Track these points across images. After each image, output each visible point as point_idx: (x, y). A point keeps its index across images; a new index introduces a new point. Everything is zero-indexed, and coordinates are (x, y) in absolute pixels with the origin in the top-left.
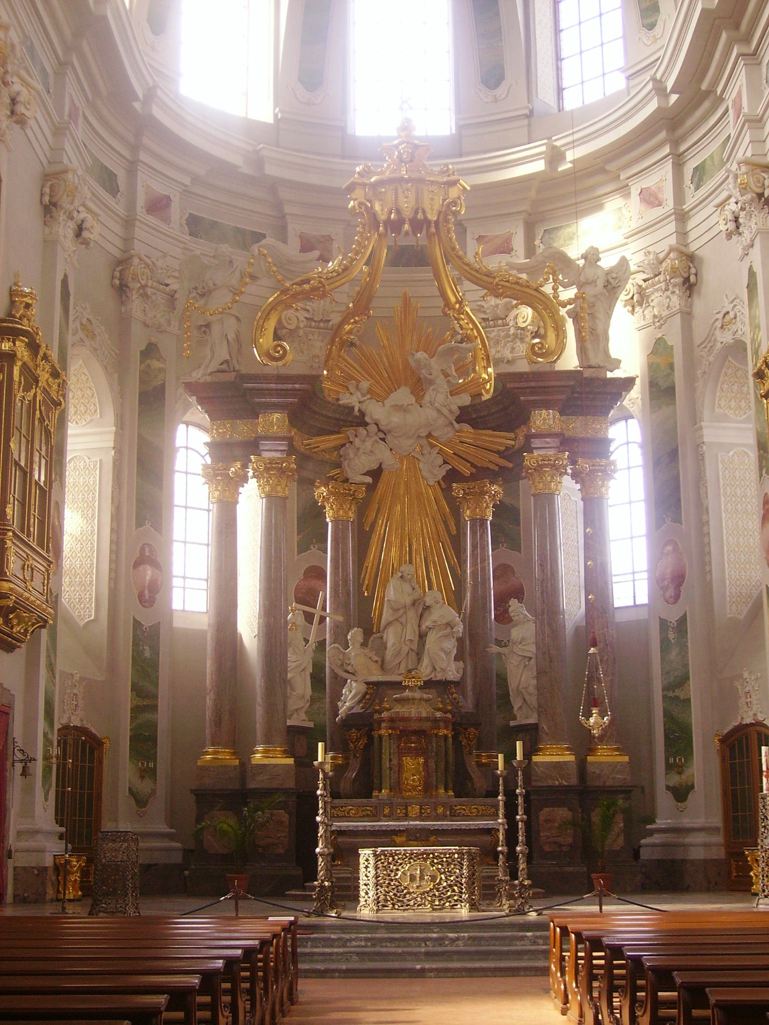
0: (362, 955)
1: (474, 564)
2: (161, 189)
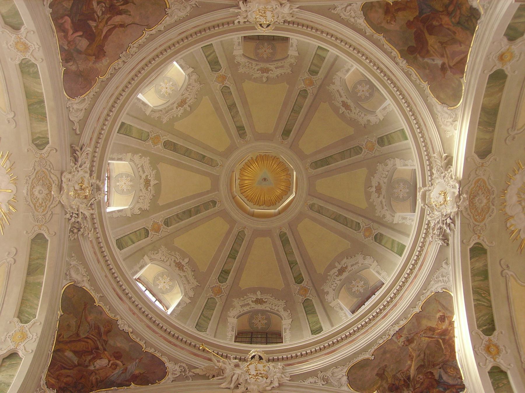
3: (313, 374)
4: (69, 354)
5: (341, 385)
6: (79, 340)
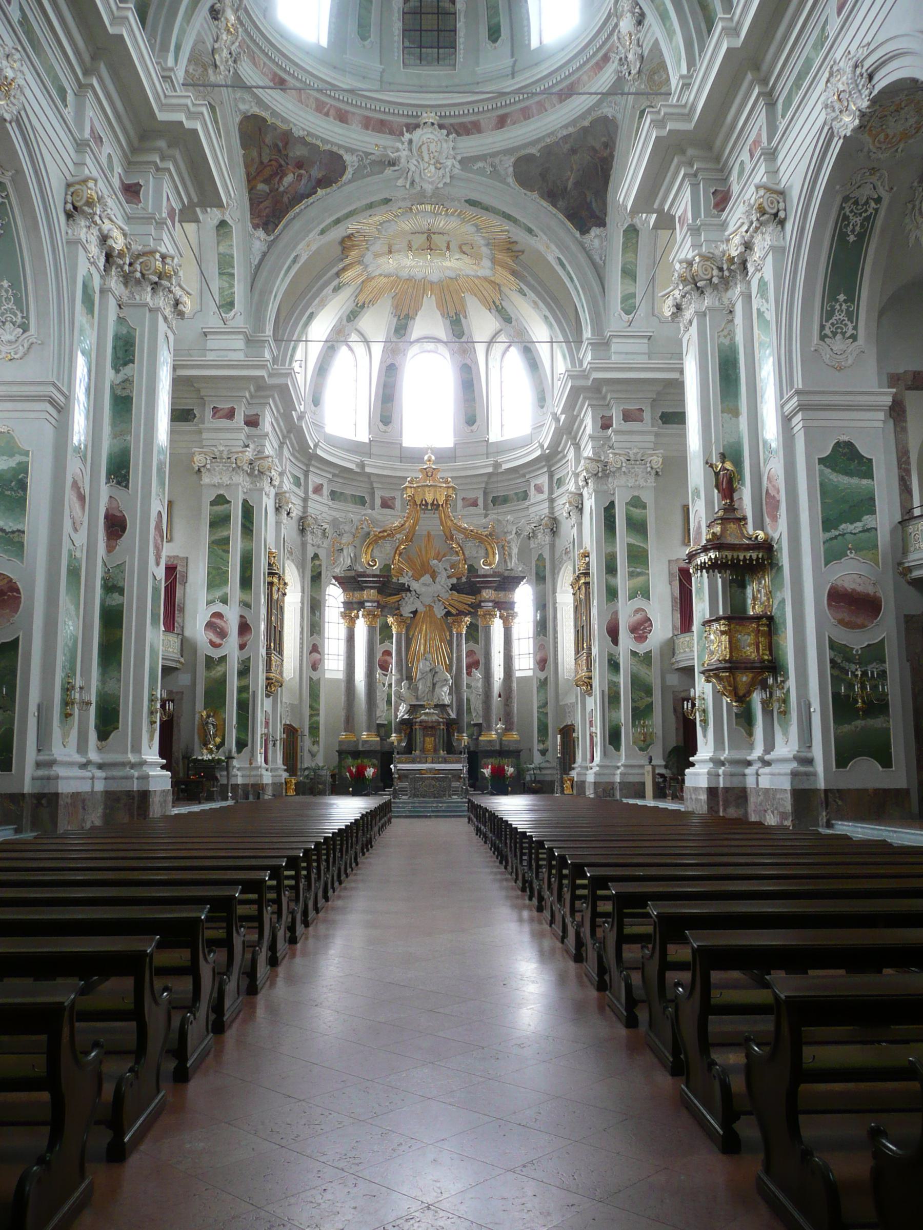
0: (410, 811)
1: (457, 653)
2: (319, 481)
3: (482, 158)
4: (261, 187)
5: (507, 176)
6: (265, 167)
